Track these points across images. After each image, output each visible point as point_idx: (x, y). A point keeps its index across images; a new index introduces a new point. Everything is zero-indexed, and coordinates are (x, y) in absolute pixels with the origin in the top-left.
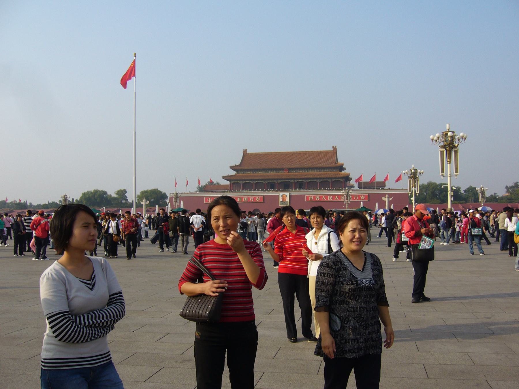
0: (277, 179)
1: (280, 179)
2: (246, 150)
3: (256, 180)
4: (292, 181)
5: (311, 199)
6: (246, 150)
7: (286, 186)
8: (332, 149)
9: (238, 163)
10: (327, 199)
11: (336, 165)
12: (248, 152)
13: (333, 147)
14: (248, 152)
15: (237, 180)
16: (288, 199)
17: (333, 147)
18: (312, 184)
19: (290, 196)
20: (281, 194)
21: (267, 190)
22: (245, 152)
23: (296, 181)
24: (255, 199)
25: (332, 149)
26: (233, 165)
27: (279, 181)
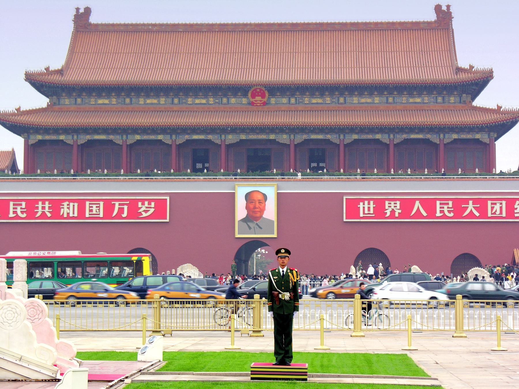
0: (223, 130)
1: (235, 129)
2: (88, 11)
3: (135, 130)
4: (284, 138)
5: (366, 209)
6: (88, 11)
7: (258, 158)
8: (432, 17)
9: (57, 64)
10: (431, 213)
11: (463, 76)
12: (94, 19)
13: (438, 8)
14: (94, 19)
15: (57, 130)
16: (270, 211)
17: (438, 8)
18: (369, 152)
19: (280, 196)
20: (241, 190)
21: (179, 171)
22: (82, 19)
23: (300, 138)
24: (134, 212)
25: (432, 17)
26: (37, 67)
27: (231, 138)
